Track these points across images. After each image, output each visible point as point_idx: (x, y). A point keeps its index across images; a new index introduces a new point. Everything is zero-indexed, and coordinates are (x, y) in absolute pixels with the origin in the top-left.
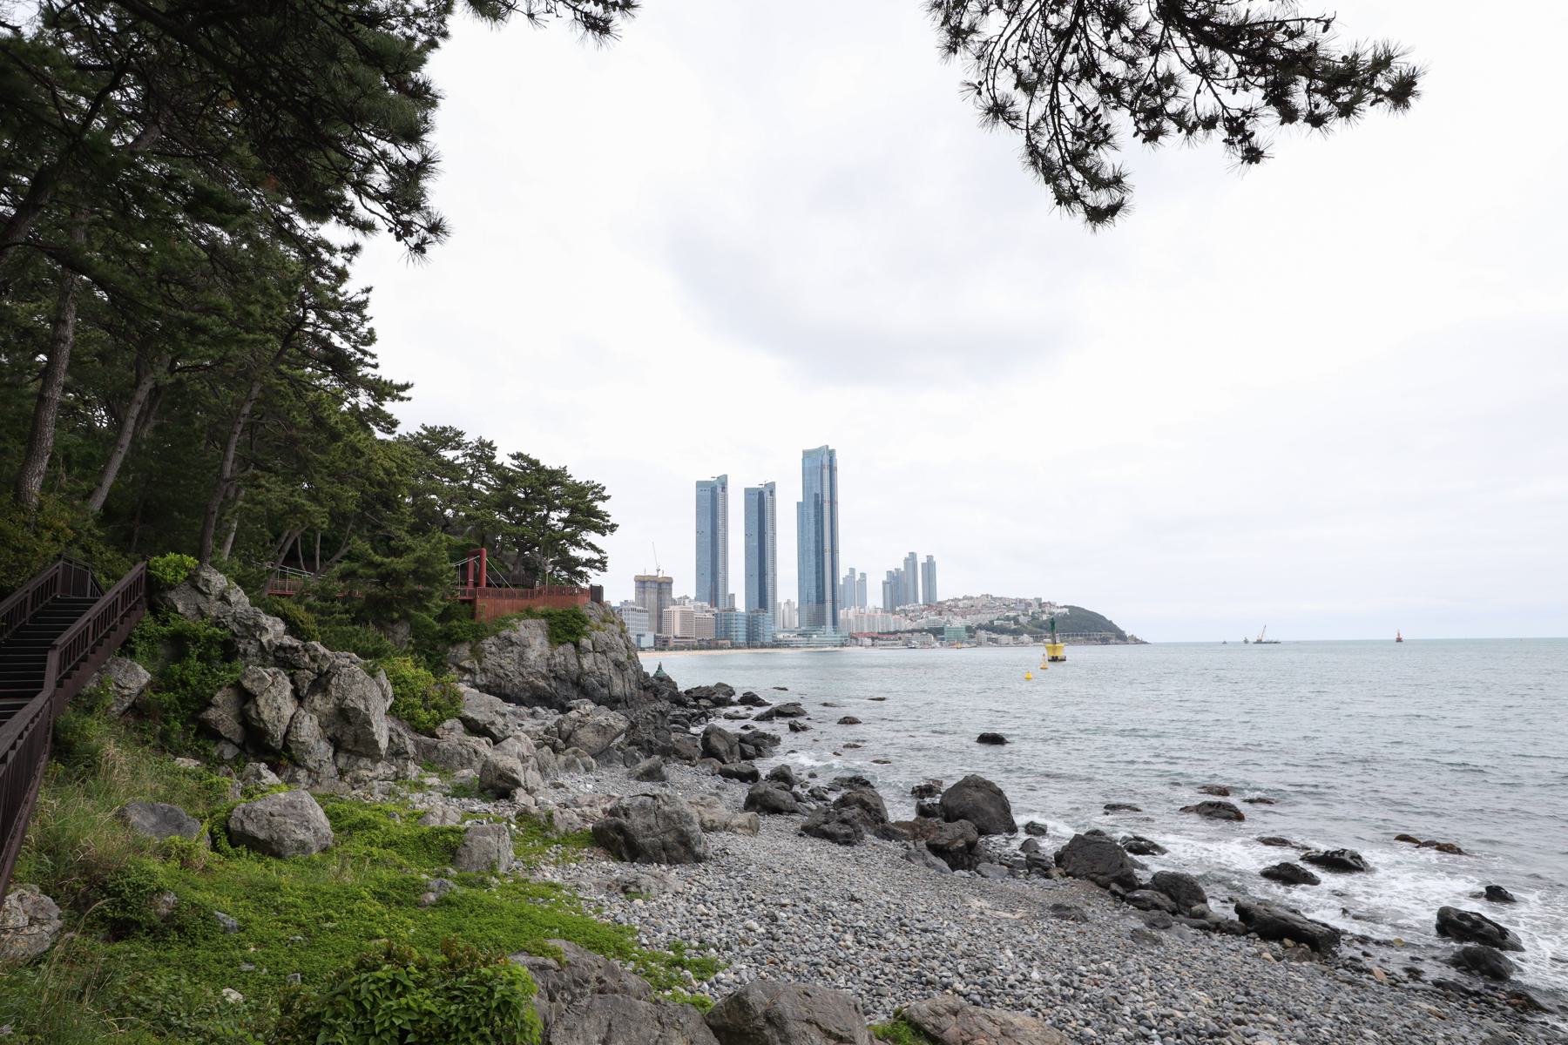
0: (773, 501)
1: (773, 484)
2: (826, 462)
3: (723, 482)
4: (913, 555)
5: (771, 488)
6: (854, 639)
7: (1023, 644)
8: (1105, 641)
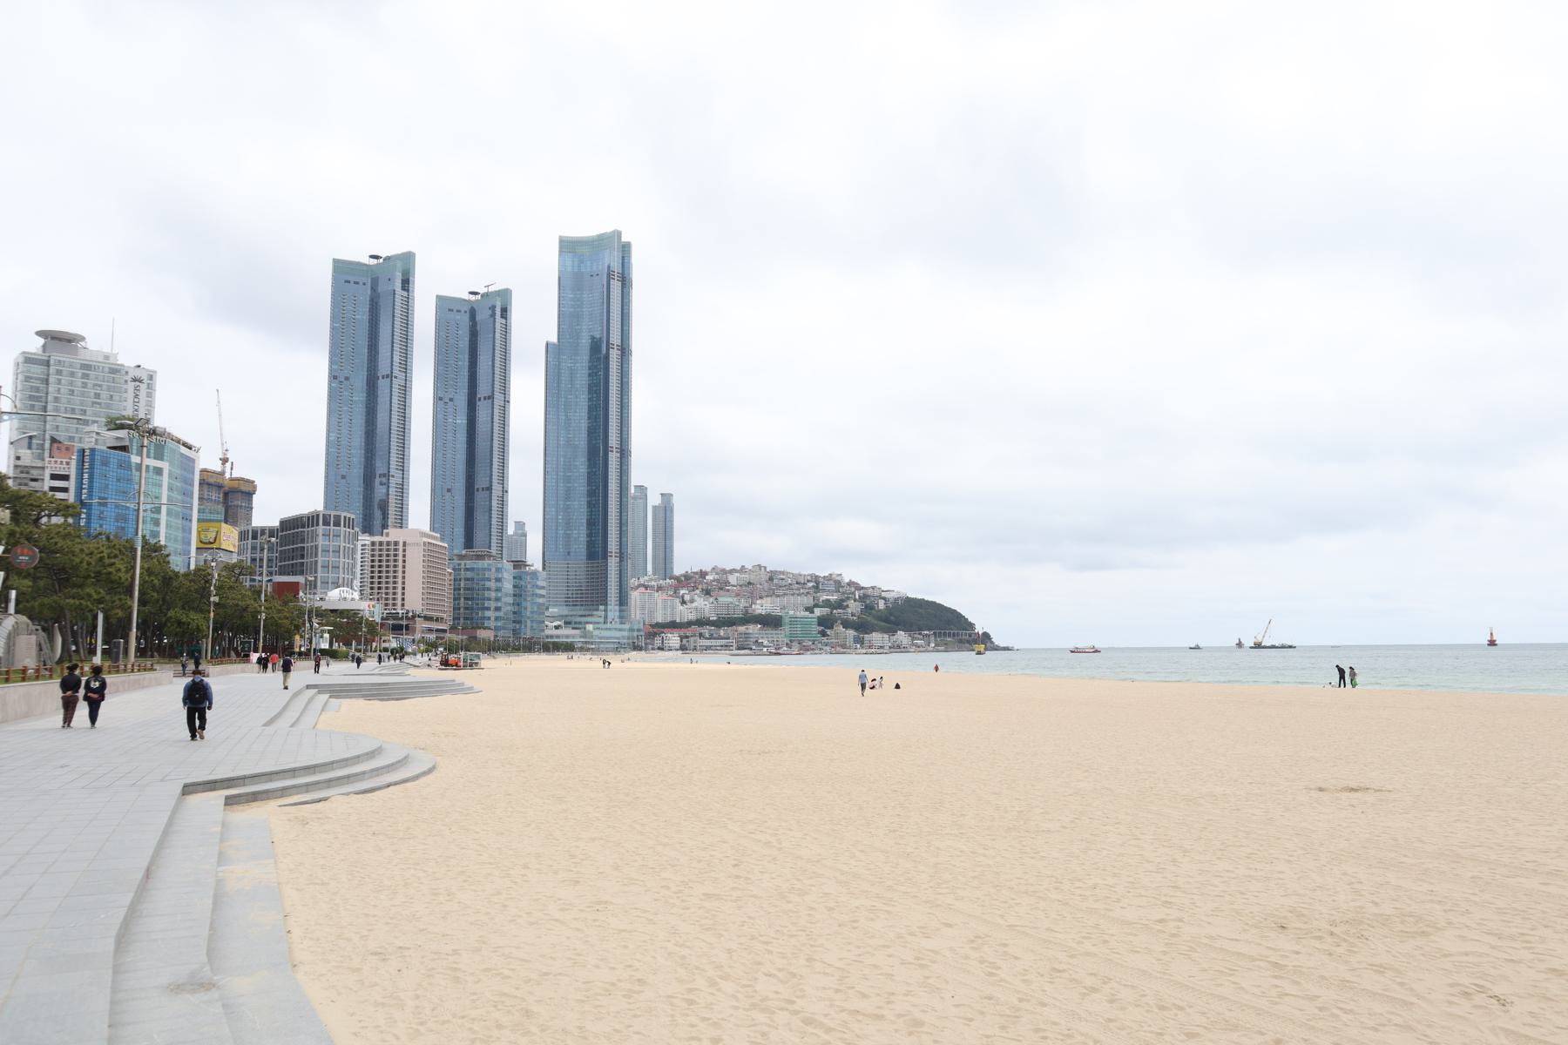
0: (506, 330)
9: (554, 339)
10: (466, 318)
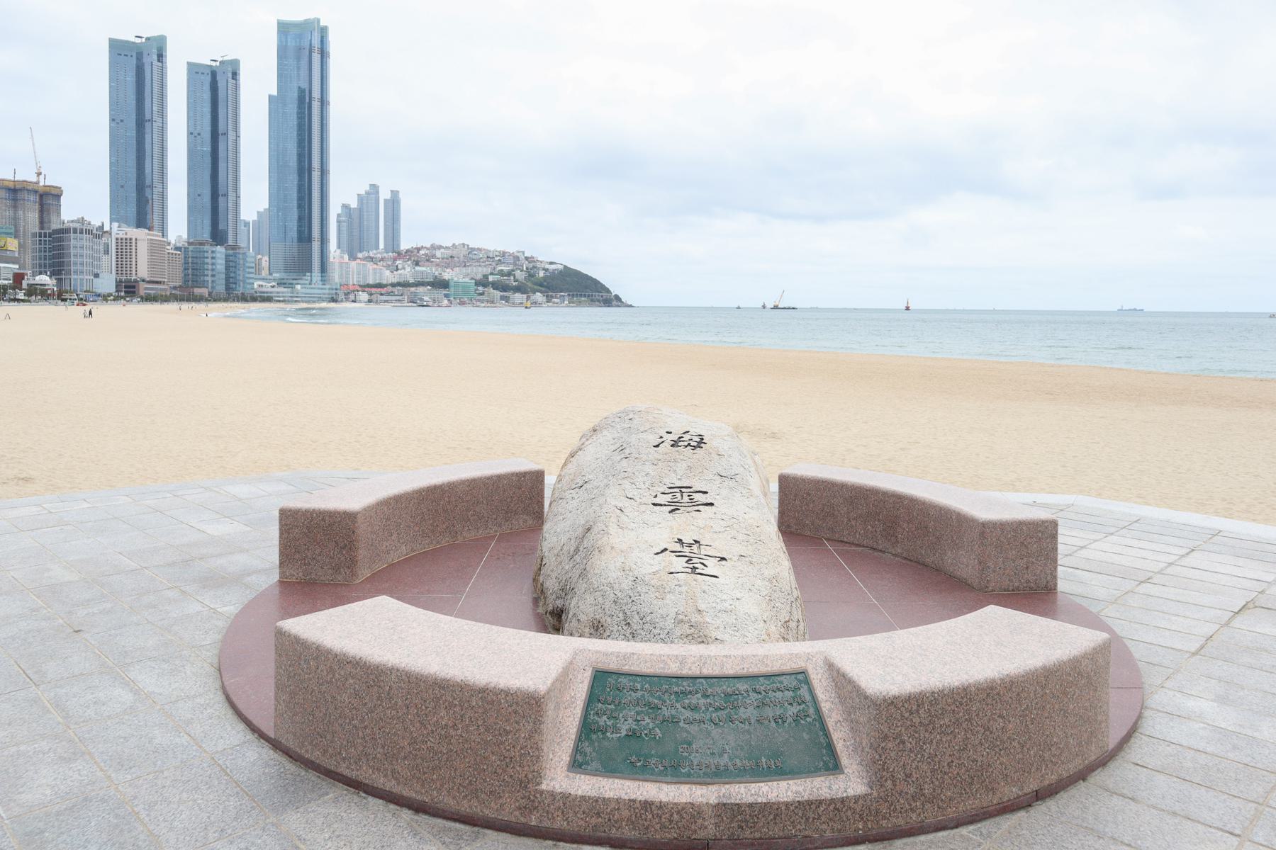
0: (236, 87)
1: (235, 63)
2: (316, 43)
3: (159, 48)
5: (233, 70)
7: (535, 303)
9: (275, 93)
10: (209, 78)
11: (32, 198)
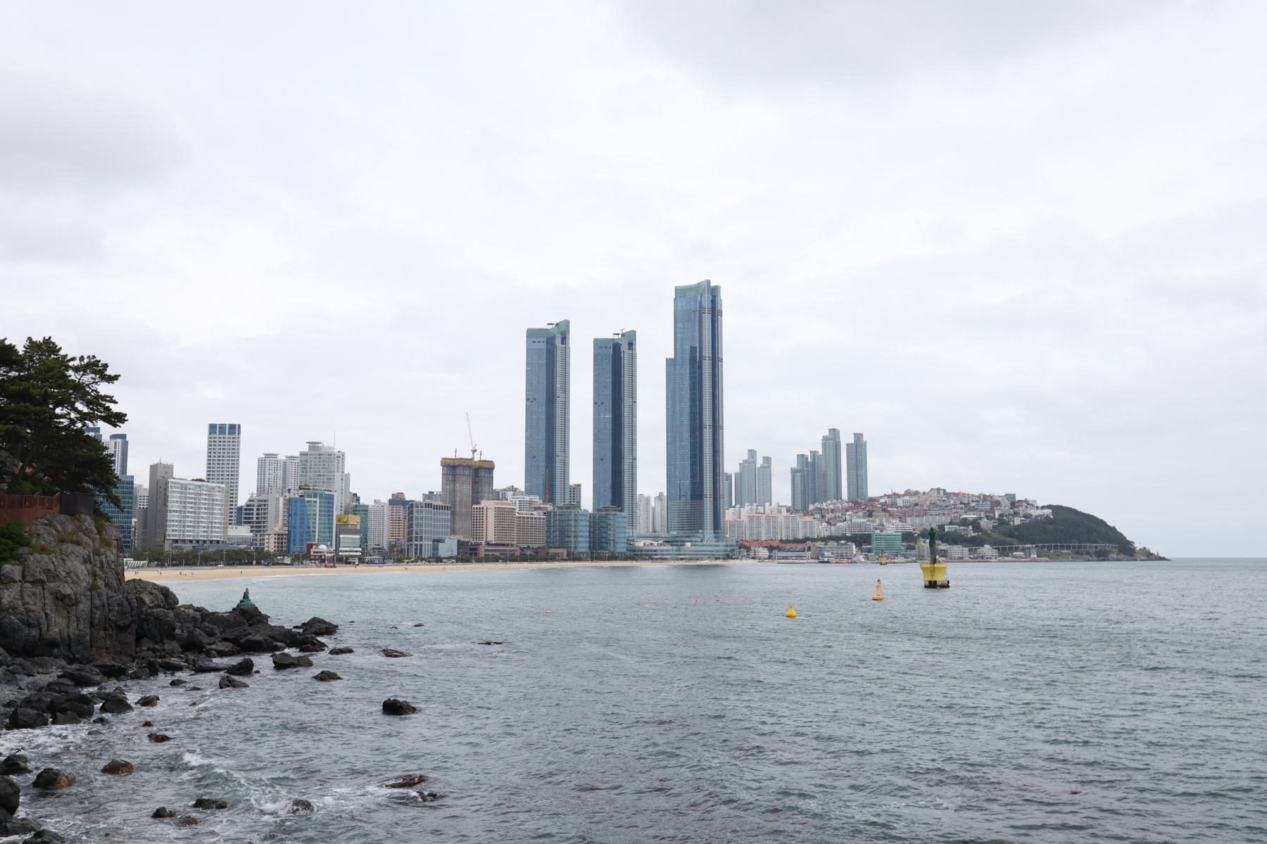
4: (834, 432)
6: (743, 549)
7: (982, 558)
8: (1102, 556)
11: (467, 472)
